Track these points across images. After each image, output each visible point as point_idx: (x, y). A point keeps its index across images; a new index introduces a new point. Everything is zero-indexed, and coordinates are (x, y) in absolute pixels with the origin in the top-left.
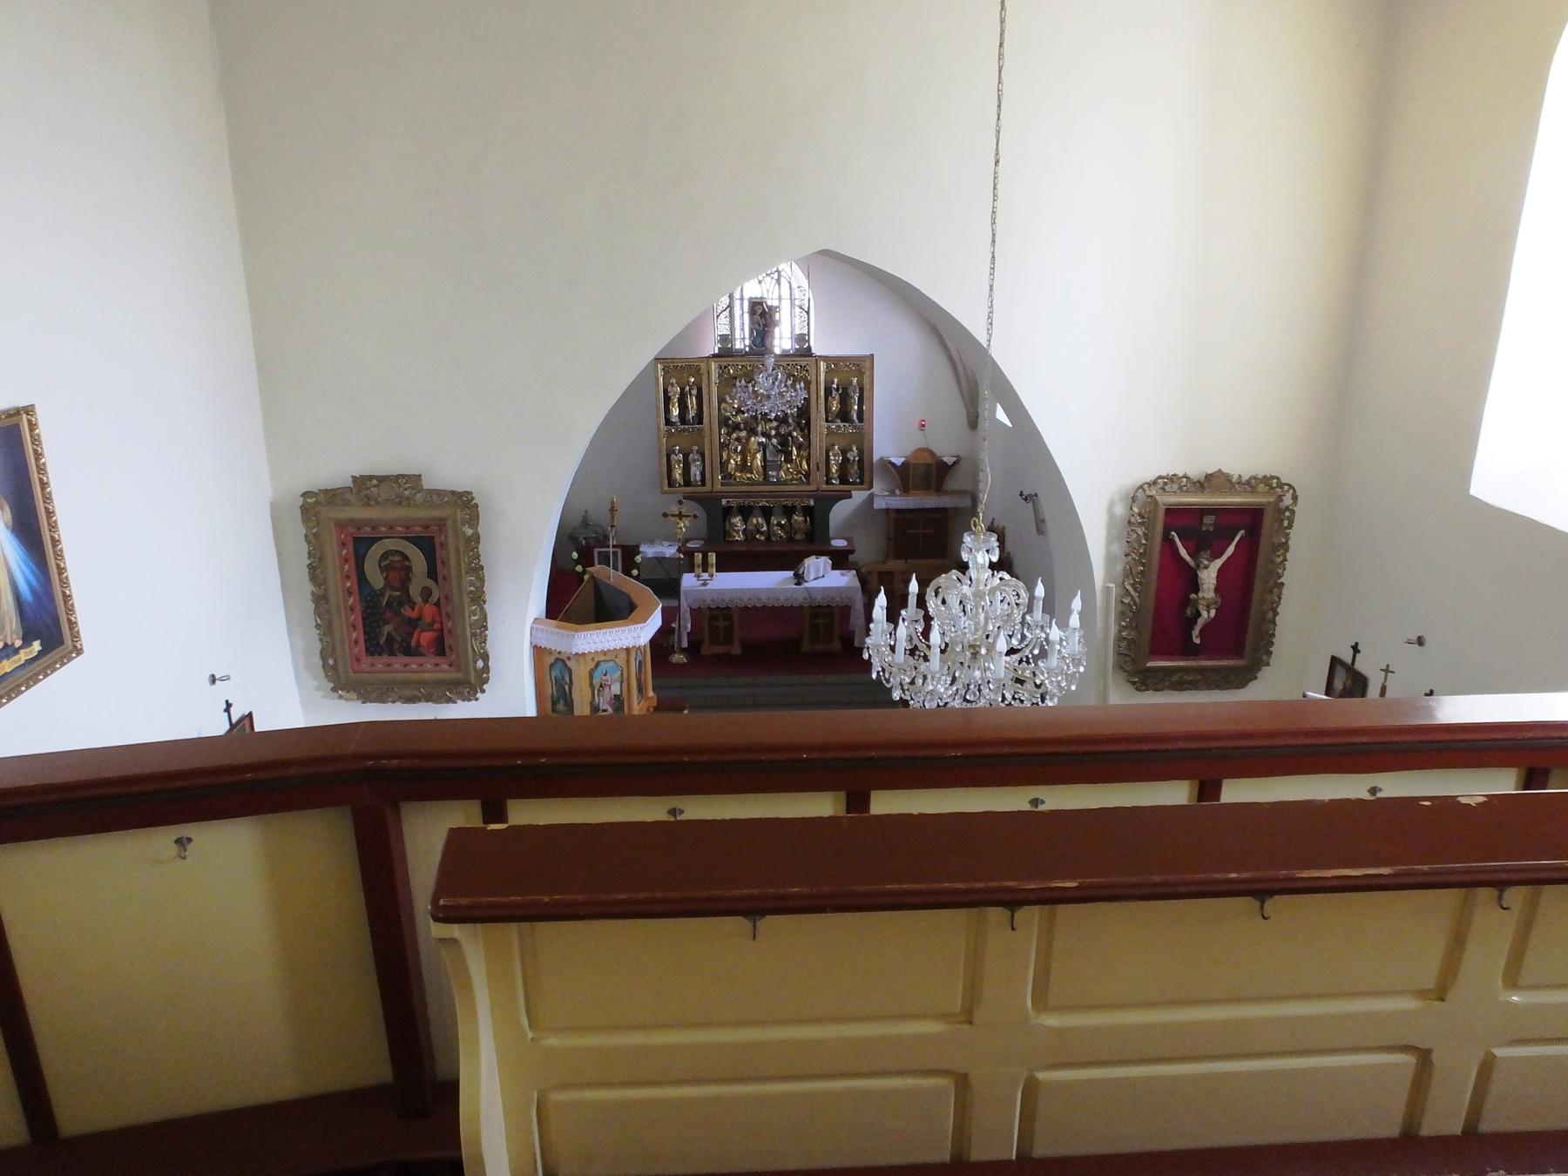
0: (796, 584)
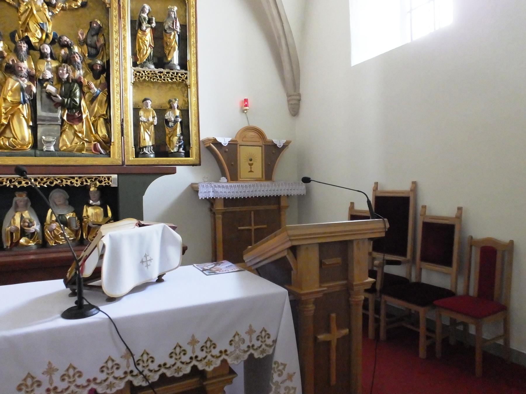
0: (68, 314)
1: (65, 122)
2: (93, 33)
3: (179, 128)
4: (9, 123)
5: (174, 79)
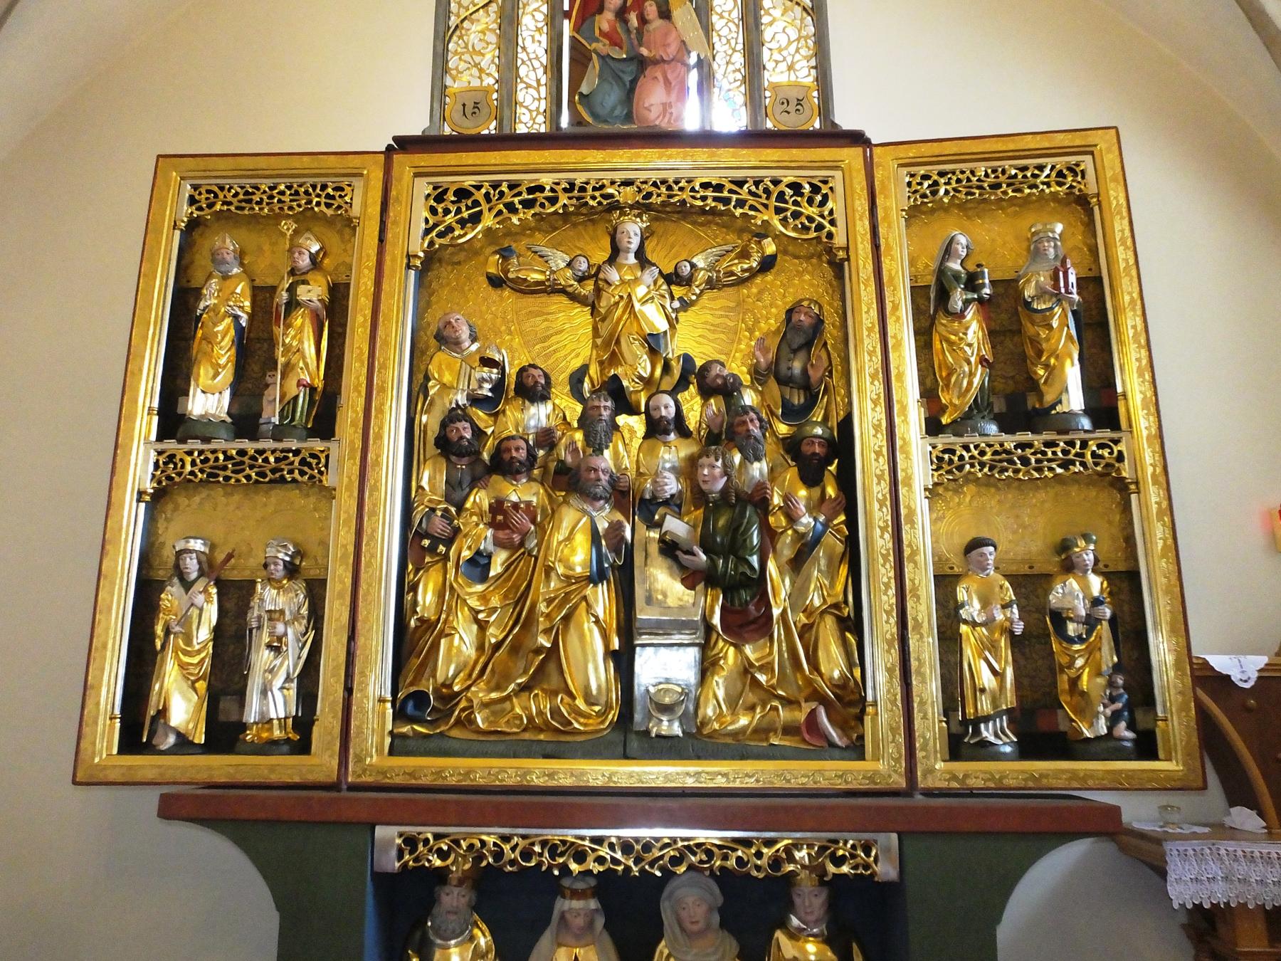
1: (714, 636)
2: (799, 340)
3: (1109, 643)
4: (555, 643)
5: (1074, 465)
